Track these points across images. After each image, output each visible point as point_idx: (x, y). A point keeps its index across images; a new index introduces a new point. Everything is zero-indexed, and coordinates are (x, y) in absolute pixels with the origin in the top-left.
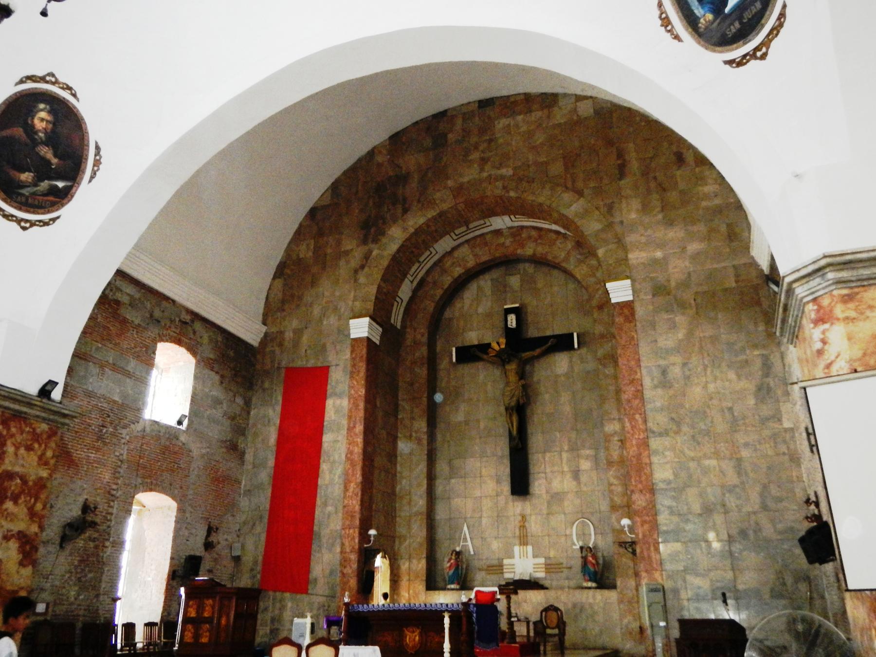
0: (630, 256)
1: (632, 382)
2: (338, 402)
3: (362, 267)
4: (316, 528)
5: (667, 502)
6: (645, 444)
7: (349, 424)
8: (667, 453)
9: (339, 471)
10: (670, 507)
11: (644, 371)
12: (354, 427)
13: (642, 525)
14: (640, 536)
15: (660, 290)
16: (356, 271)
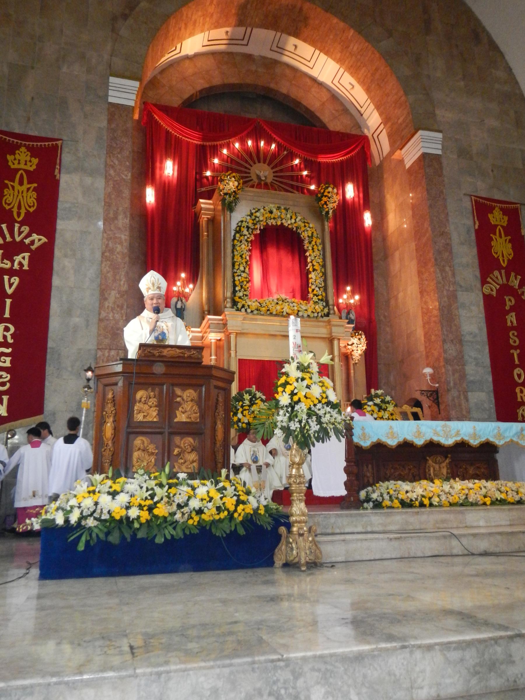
0: (438, 112)
1: (442, 234)
2: (88, 180)
3: (125, 17)
4: (50, 344)
5: (473, 354)
6: (453, 297)
7: (106, 212)
8: (473, 308)
9: (92, 272)
10: (475, 359)
11: (452, 227)
12: (116, 218)
14: (452, 384)
15: (463, 153)
16: (114, 19)
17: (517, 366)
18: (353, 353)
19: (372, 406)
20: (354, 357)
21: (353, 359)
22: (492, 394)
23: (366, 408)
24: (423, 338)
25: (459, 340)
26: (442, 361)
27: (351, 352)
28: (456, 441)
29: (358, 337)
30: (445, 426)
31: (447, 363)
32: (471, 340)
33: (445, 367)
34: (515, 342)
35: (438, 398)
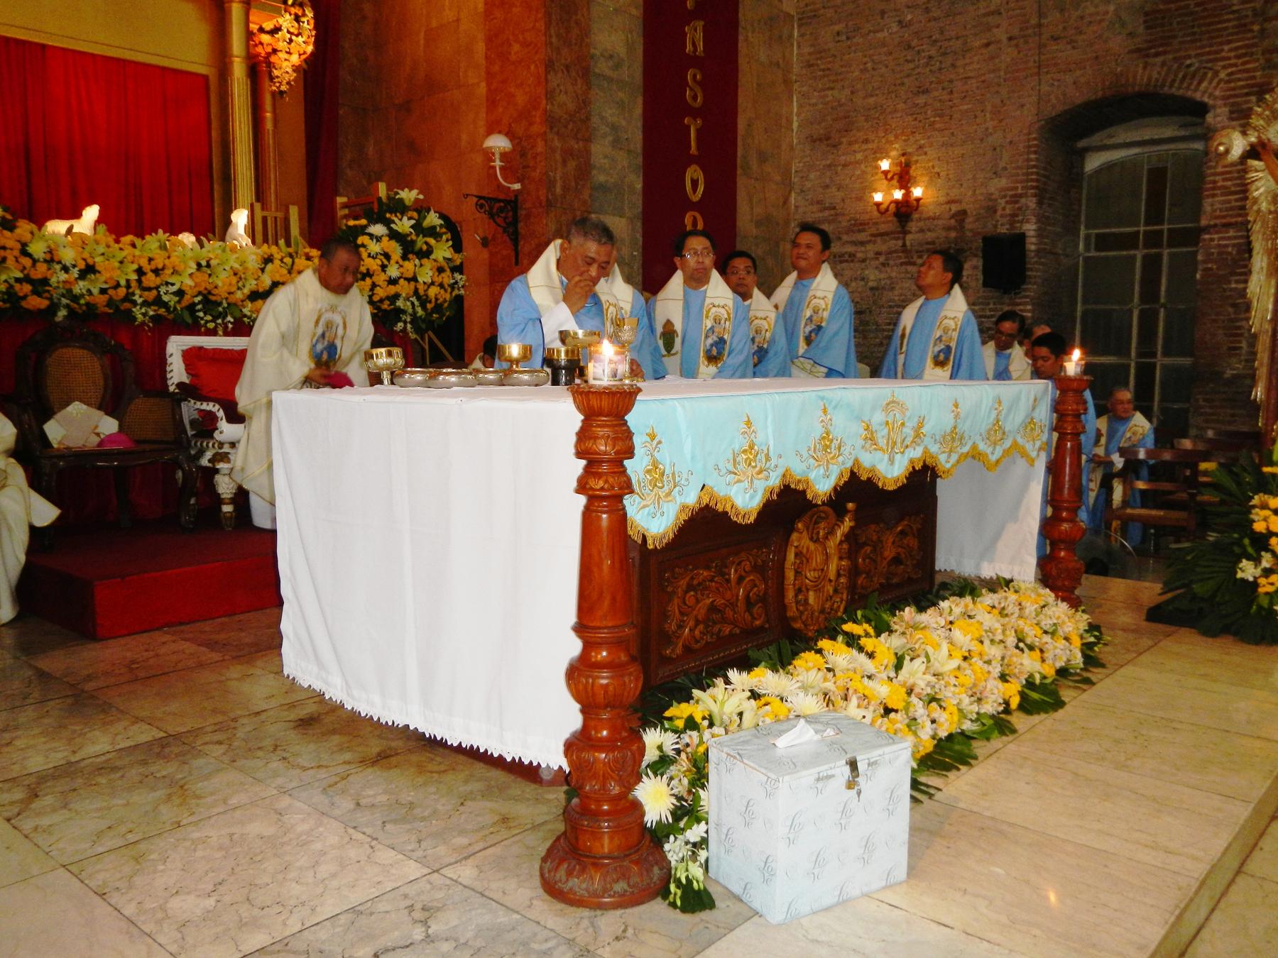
5: (610, 113)
10: (614, 128)
13: (564, 162)
14: (558, 190)
17: (691, 160)
18: (273, 59)
19: (385, 239)
20: (276, 73)
21: (272, 78)
22: (639, 225)
23: (363, 246)
24: (480, 47)
25: (583, 69)
26: (538, 120)
27: (269, 55)
28: (911, 461)
29: (293, 10)
30: (892, 404)
31: (551, 128)
32: (608, 73)
33: (546, 141)
34: (695, 98)
35: (515, 221)
